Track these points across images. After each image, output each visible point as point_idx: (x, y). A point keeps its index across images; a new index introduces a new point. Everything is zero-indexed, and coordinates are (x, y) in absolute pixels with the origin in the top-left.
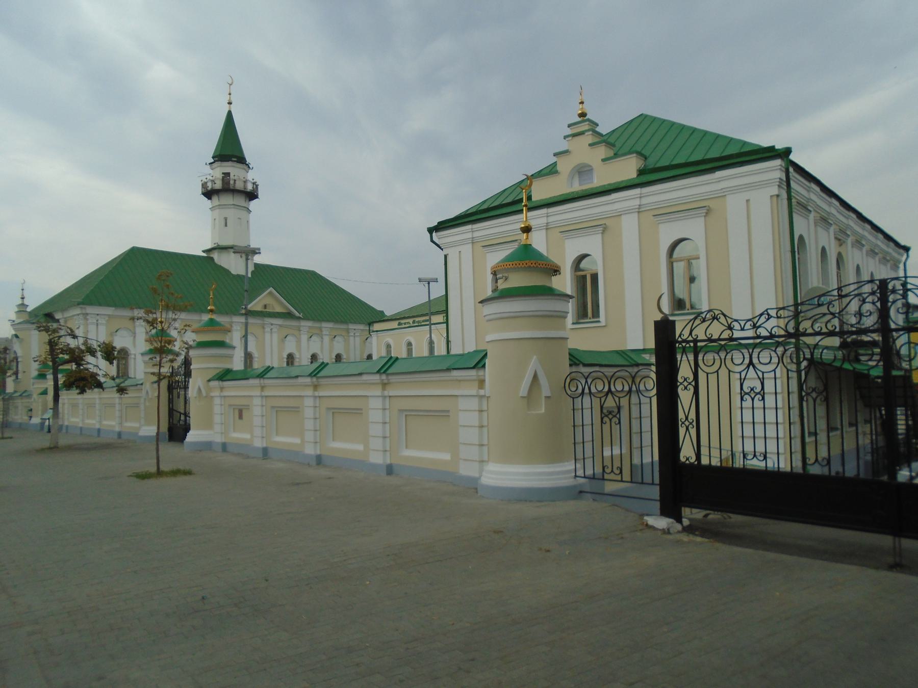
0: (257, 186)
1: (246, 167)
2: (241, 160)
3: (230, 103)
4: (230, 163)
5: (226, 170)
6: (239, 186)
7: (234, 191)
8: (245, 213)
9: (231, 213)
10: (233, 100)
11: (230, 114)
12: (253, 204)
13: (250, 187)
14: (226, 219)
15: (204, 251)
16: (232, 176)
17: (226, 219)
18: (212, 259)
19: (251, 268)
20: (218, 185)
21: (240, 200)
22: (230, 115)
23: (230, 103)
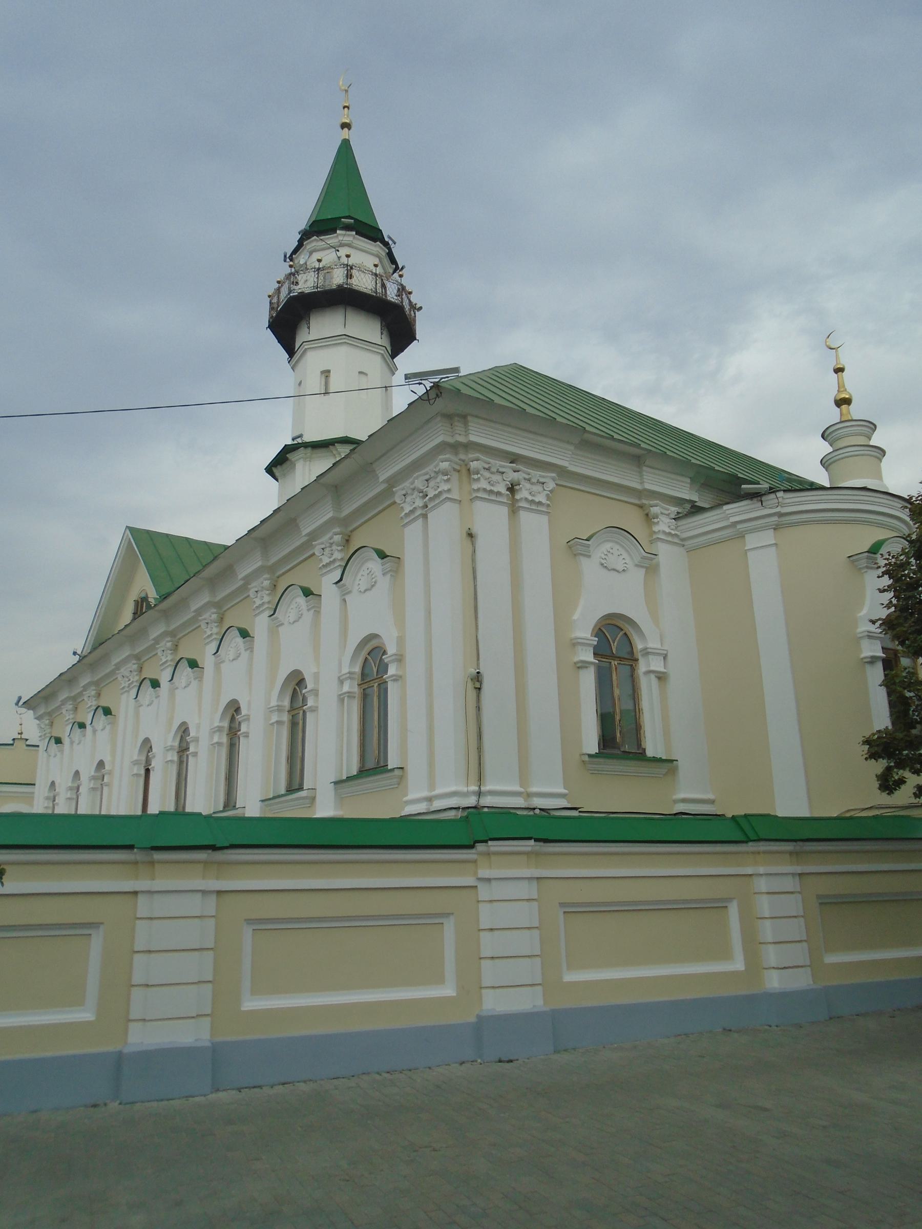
1: (383, 252)
2: (371, 233)
6: (364, 283)
11: (346, 146)
21: (369, 330)
22: (345, 151)
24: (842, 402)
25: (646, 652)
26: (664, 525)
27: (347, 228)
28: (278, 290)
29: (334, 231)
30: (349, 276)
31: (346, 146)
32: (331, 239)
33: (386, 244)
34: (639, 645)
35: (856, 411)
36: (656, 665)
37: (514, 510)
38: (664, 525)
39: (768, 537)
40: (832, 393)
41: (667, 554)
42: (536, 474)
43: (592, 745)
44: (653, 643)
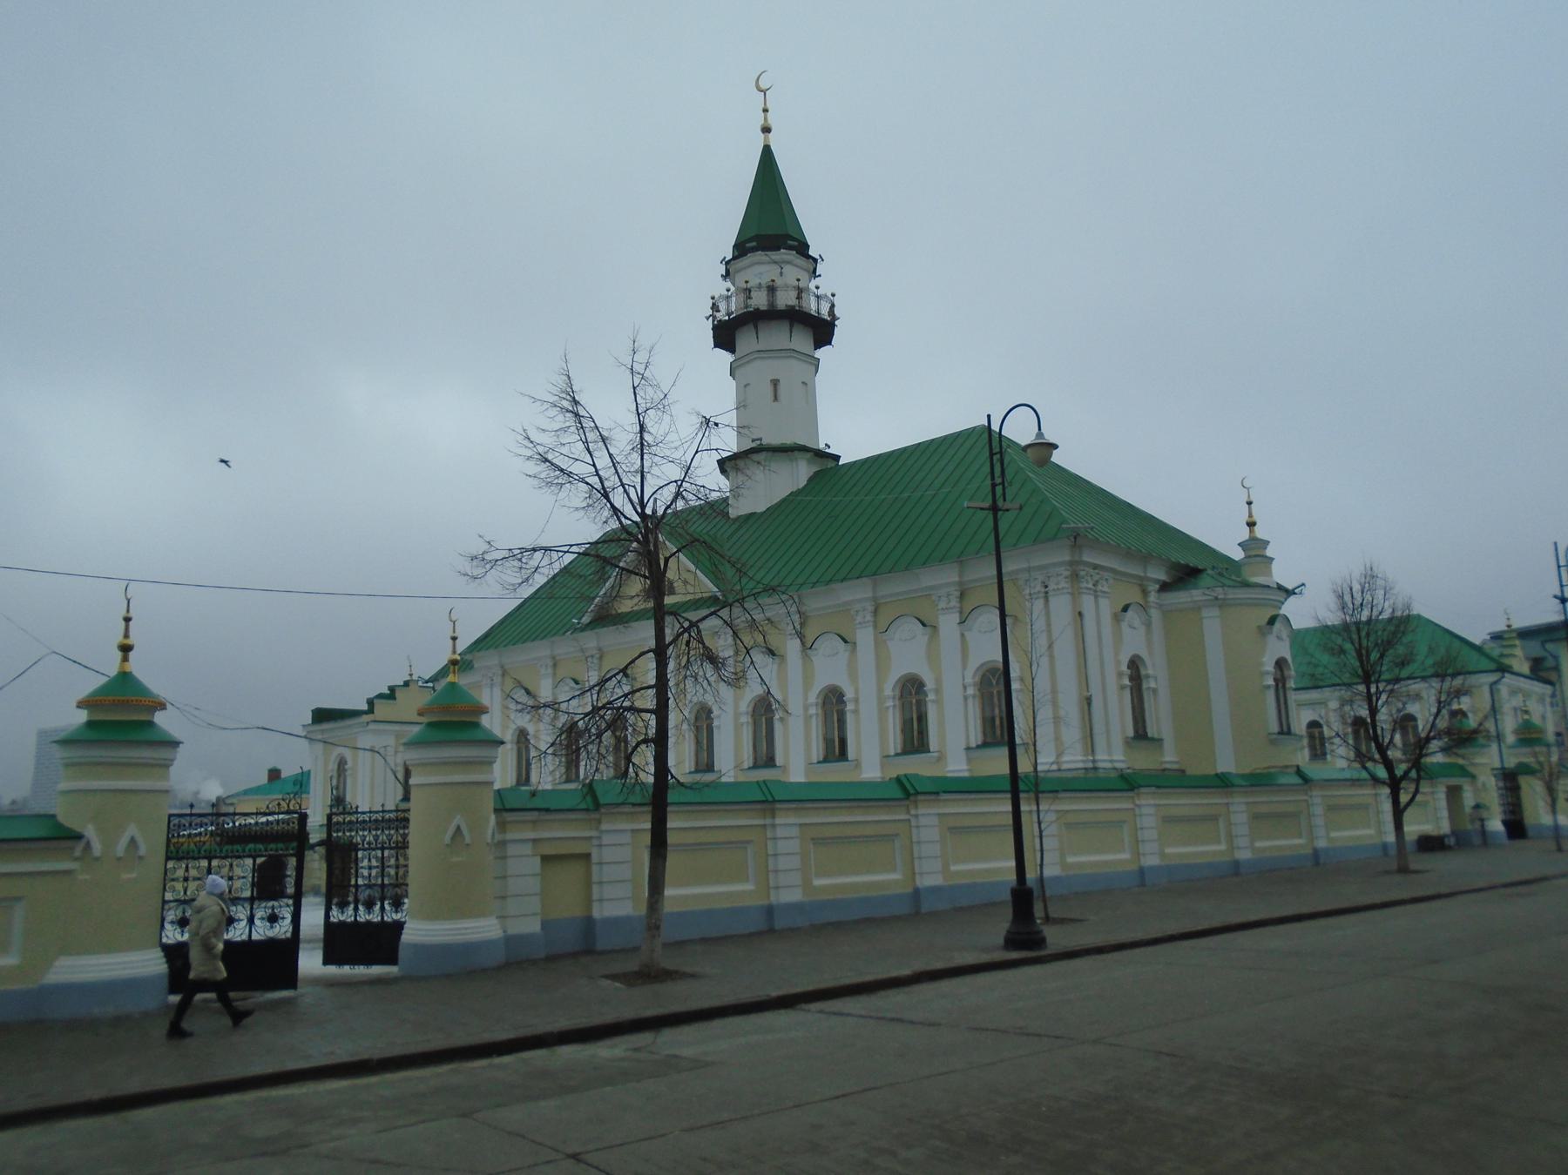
2: (802, 248)
3: (766, 130)
4: (784, 254)
9: (789, 371)
10: (772, 122)
12: (822, 353)
14: (775, 383)
17: (775, 383)
21: (801, 340)
23: (766, 130)
24: (1251, 524)
25: (1148, 676)
26: (1153, 597)
27: (791, 248)
29: (778, 249)
30: (799, 298)
31: (767, 155)
32: (775, 255)
33: (815, 260)
34: (1143, 672)
35: (1260, 532)
36: (1153, 685)
37: (1096, 597)
38: (1153, 597)
39: (1215, 612)
40: (1246, 518)
41: (1154, 613)
42: (1106, 575)
43: (1131, 733)
44: (1150, 672)
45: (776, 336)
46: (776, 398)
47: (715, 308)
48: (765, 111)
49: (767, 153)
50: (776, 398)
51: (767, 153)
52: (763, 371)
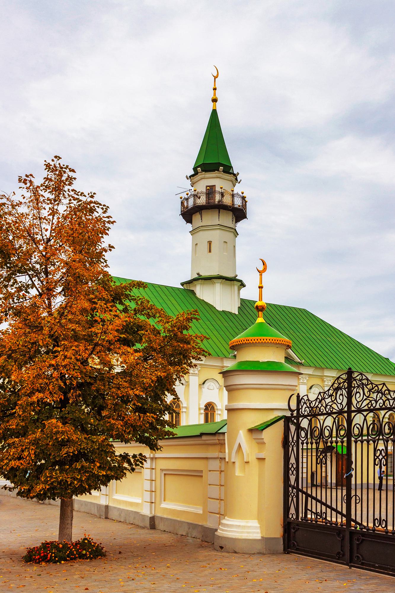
0: (246, 202)
1: (233, 178)
2: (228, 169)
3: (215, 100)
5: (211, 182)
6: (227, 200)
7: (221, 207)
8: (232, 235)
9: (216, 236)
12: (241, 226)
13: (238, 202)
14: (210, 243)
15: (182, 284)
16: (218, 189)
17: (210, 243)
18: (193, 292)
19: (238, 304)
20: (202, 201)
21: (227, 219)
23: (215, 100)
28: (187, 199)
45: (210, 219)
46: (210, 251)
47: (182, 203)
48: (215, 89)
49: (214, 113)
50: (210, 251)
51: (214, 113)
52: (205, 236)
